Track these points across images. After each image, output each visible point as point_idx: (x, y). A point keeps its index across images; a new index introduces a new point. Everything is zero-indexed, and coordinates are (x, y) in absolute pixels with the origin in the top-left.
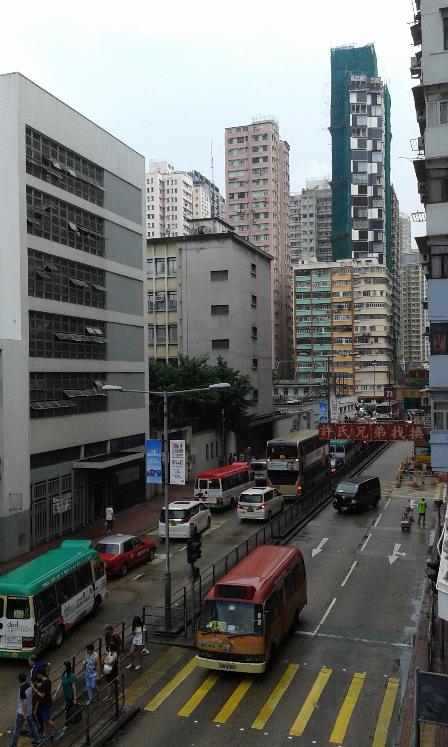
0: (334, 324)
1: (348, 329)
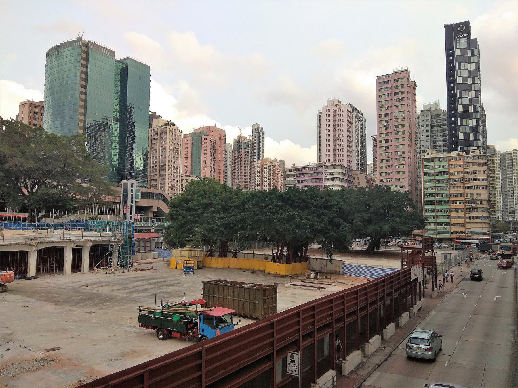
0: (451, 192)
1: (462, 195)
